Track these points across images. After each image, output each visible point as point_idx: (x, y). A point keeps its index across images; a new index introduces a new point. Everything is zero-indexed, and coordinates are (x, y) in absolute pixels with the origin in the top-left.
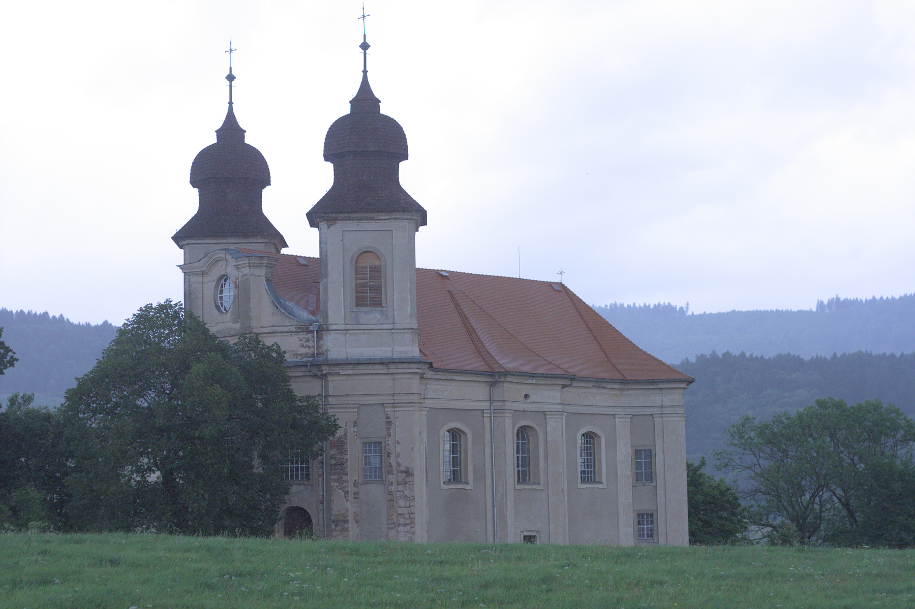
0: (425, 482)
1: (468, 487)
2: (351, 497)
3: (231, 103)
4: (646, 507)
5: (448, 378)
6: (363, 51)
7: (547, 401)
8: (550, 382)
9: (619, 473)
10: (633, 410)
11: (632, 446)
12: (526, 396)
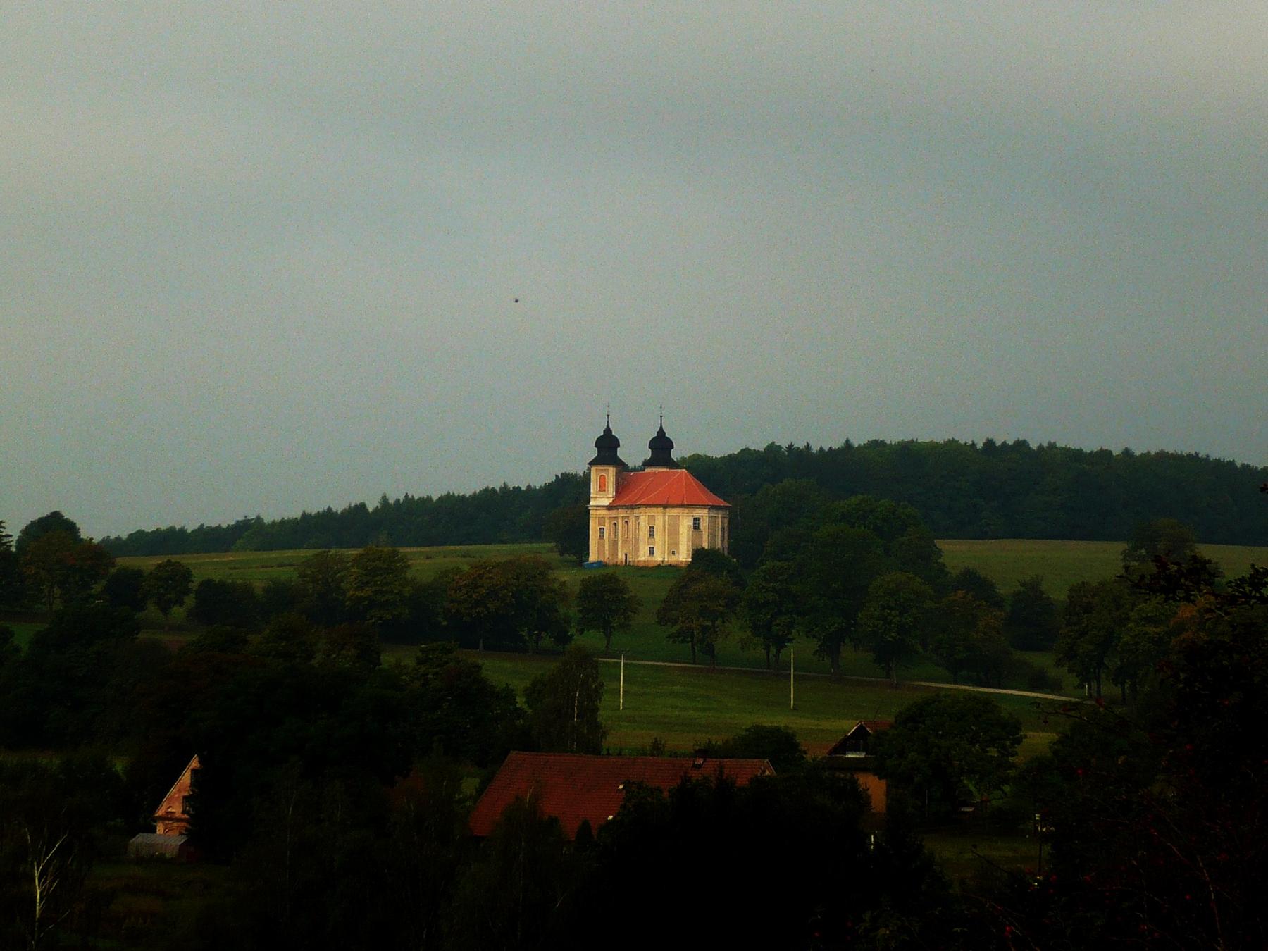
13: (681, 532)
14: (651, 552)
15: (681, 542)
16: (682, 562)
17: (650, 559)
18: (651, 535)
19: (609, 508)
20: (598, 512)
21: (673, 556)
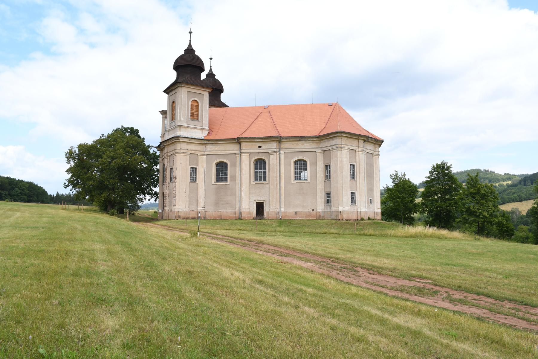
1: (228, 183)
2: (168, 187)
3: (211, 66)
4: (328, 190)
5: (215, 142)
7: (270, 148)
9: (318, 176)
10: (324, 148)
11: (324, 164)
14: (353, 202)
15: (375, 189)
17: (353, 208)
18: (353, 176)
19: (204, 142)
20: (190, 147)
21: (371, 206)
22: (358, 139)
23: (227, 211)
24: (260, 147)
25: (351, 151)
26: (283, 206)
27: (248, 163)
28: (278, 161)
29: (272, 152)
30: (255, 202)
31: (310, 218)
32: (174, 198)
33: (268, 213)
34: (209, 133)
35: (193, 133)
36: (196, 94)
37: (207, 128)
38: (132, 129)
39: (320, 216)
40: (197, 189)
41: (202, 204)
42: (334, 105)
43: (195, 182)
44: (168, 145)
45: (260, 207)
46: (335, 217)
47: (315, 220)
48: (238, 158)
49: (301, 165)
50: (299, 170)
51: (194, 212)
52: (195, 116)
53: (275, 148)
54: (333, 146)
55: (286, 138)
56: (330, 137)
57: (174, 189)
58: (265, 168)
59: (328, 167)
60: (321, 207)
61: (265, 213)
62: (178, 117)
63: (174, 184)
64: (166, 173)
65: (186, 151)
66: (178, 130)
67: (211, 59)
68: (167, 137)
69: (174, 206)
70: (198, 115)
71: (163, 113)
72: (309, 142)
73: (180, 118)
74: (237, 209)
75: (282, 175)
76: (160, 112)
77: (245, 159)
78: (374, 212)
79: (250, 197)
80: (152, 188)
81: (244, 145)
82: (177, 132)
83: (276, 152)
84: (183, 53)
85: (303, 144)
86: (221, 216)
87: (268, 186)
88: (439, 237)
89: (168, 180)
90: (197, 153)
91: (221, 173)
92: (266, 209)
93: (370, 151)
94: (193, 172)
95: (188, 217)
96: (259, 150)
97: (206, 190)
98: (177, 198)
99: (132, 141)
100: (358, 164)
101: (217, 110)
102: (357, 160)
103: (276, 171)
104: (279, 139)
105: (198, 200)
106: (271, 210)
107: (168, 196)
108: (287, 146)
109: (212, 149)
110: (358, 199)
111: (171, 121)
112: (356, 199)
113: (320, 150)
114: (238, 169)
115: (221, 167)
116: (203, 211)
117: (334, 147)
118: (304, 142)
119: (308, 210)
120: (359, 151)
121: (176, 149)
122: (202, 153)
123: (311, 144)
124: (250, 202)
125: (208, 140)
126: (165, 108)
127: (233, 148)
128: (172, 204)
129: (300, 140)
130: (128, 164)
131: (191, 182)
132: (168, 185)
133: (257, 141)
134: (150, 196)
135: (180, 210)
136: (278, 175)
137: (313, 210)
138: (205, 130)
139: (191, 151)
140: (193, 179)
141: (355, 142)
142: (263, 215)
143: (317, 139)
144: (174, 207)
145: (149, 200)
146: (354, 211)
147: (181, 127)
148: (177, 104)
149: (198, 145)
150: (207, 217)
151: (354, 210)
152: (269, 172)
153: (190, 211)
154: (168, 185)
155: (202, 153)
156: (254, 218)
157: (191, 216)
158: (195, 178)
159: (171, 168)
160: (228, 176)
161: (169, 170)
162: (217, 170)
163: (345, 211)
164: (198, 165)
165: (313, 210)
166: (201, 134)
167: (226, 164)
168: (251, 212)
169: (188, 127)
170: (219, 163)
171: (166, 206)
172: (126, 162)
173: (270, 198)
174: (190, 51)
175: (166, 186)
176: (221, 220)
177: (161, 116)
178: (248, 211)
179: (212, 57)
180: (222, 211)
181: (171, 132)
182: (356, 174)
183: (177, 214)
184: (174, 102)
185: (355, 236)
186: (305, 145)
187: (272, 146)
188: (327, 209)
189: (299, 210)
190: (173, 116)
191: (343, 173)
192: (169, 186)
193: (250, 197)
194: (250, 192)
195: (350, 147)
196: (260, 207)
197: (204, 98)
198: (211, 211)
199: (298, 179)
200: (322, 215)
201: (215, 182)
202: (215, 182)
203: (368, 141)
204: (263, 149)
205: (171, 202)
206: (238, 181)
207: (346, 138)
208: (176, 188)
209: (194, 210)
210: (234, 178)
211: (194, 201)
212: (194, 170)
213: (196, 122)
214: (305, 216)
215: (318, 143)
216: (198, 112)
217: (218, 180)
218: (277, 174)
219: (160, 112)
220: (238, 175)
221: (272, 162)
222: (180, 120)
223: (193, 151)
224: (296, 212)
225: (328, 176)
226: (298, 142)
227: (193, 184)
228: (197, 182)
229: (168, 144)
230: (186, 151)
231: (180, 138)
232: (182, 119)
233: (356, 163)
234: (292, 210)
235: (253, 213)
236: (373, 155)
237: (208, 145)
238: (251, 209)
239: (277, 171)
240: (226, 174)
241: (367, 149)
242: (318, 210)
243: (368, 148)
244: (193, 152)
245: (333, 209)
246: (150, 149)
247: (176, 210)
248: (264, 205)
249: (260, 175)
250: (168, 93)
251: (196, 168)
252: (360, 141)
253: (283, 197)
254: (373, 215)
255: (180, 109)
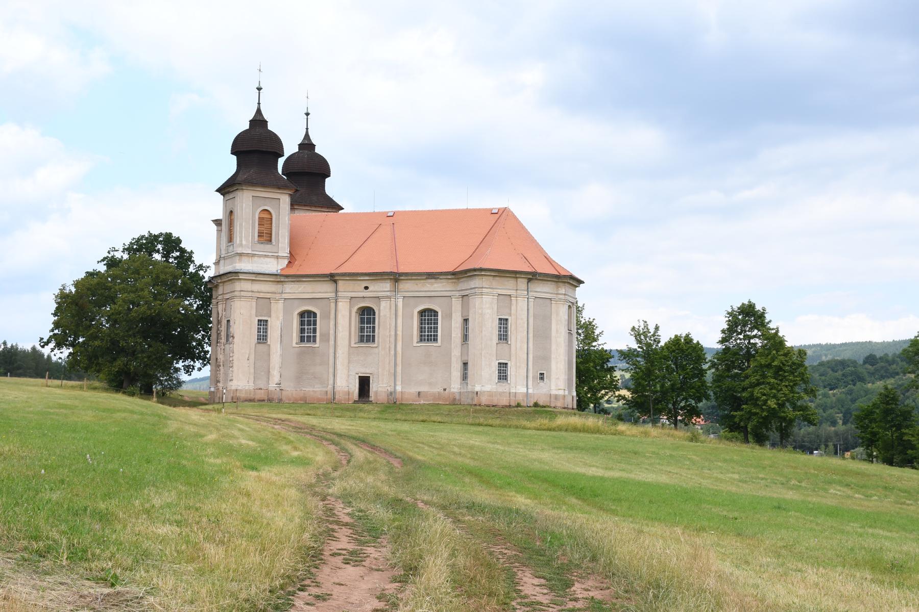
0: (279, 342)
2: (222, 351)
4: (465, 358)
5: (298, 280)
6: (258, 91)
8: (380, 278)
9: (453, 335)
10: (463, 292)
11: (462, 316)
12: (366, 288)
13: (554, 334)
15: (553, 356)
16: (556, 397)
18: (503, 336)
19: (279, 278)
20: (257, 287)
21: (542, 384)
22: (517, 278)
23: (314, 389)
24: (366, 288)
25: (502, 297)
26: (399, 382)
27: (348, 314)
28: (393, 311)
29: (384, 297)
30: (357, 376)
31: (440, 403)
32: (231, 369)
33: (376, 393)
34: (290, 262)
35: (261, 264)
36: (267, 200)
37: (286, 255)
38: (168, 236)
39: (455, 399)
40: (269, 355)
41: (275, 377)
42: (500, 213)
43: (264, 343)
44: (224, 282)
45: (364, 383)
46: (469, 401)
47: (447, 405)
48: (333, 305)
49: (428, 317)
50: (427, 326)
51: (262, 391)
52: (266, 235)
53: (388, 291)
54: (472, 290)
55: (406, 274)
56: (468, 275)
57: (231, 355)
58: (374, 323)
59: (466, 321)
60: (455, 386)
61: (372, 393)
62: (237, 240)
63: (231, 346)
64: (221, 327)
65: (250, 294)
66: (238, 261)
67: (307, 114)
68: (223, 269)
69: (230, 381)
70: (271, 234)
71: (218, 222)
72: (441, 281)
73: (241, 241)
74: (330, 387)
75: (400, 333)
76: (212, 220)
77: (343, 307)
78: (550, 394)
79: (349, 367)
80: (205, 347)
81: (340, 283)
82: (235, 263)
83: (389, 297)
84: (246, 126)
85: (432, 284)
86: (306, 397)
87: (377, 349)
88: (585, 430)
89: (223, 340)
90: (268, 296)
91: (308, 328)
92: (374, 387)
93: (542, 294)
94: (262, 327)
95: (252, 399)
96: (367, 294)
97: (282, 355)
98: (235, 368)
99: (166, 274)
100: (513, 317)
101: (311, 218)
102: (513, 312)
103: (389, 327)
104: (396, 278)
105: (269, 372)
106: (380, 389)
107: (223, 366)
108: (407, 286)
109: (293, 290)
110: (513, 373)
111: (228, 243)
112: (509, 373)
113: (457, 294)
114: (332, 323)
115: (308, 318)
116: (278, 389)
117: (473, 291)
118: (433, 281)
119: (438, 389)
120: (517, 297)
121: (234, 291)
122: (278, 297)
123: (445, 284)
124: (348, 376)
125: (287, 276)
126: (220, 215)
127: (324, 290)
128: (228, 379)
129: (427, 279)
130: (158, 314)
131: (259, 343)
132: (223, 347)
133: (362, 278)
134: (201, 361)
135: (239, 388)
136: (393, 333)
137: (445, 390)
138: (283, 257)
139: (258, 294)
140: (262, 338)
141: (510, 281)
142: (368, 396)
143: (453, 277)
144: (230, 383)
145: (200, 369)
146: (504, 392)
147: (241, 255)
148: (236, 214)
149: (270, 283)
150: (284, 399)
151: (505, 391)
152: (379, 328)
153: (257, 389)
154: (223, 347)
155: (278, 297)
156: (355, 402)
157: (258, 397)
158: (266, 336)
159: (228, 319)
160: (318, 334)
161: (224, 322)
162: (302, 323)
163: (484, 392)
164: (270, 316)
165: (445, 390)
166: (276, 266)
167: (315, 315)
168: (351, 391)
169: (253, 255)
170: (304, 313)
171: (219, 382)
172: (155, 311)
173: (380, 370)
174: (258, 122)
175: (221, 349)
176: (305, 404)
177: (214, 227)
178: (346, 389)
179: (309, 112)
180: (307, 390)
181: (227, 261)
182: (509, 333)
183: (235, 395)
184: (231, 212)
185: (467, 427)
186: (436, 285)
187: (383, 288)
188: (464, 388)
189: (423, 389)
190: (231, 235)
191: (483, 332)
192: (224, 350)
193: (349, 367)
194: (349, 360)
195: (500, 291)
196: (364, 383)
197: (281, 205)
198: (290, 389)
199: (425, 340)
200: (457, 397)
201: (297, 344)
202: (297, 344)
203: (537, 279)
204: (371, 292)
205: (226, 374)
206: (332, 342)
207: (491, 278)
208: (233, 353)
209: (262, 387)
210: (325, 337)
211: (263, 373)
212: (263, 324)
213: (268, 247)
214: (432, 398)
215: (455, 283)
216: (271, 229)
217: (302, 339)
218: (390, 332)
219: (212, 220)
220: (332, 332)
221: (383, 311)
222: (241, 245)
223: (261, 294)
224: (419, 393)
225: (465, 337)
226: (424, 281)
227: (261, 347)
228: (269, 343)
229: (223, 280)
230: (250, 294)
231: (239, 275)
232: (244, 242)
233: (511, 316)
234: (413, 390)
235: (353, 392)
236: (551, 301)
237: (287, 283)
238: (351, 386)
239: (390, 327)
240: (315, 330)
241: (536, 292)
242: (452, 390)
243: (539, 290)
244: (262, 295)
245: (470, 388)
246: (205, 272)
247: (234, 388)
248: (371, 381)
249: (367, 332)
250: (223, 194)
251: (267, 321)
252: (519, 280)
253: (399, 369)
254: (548, 399)
255: (241, 225)
